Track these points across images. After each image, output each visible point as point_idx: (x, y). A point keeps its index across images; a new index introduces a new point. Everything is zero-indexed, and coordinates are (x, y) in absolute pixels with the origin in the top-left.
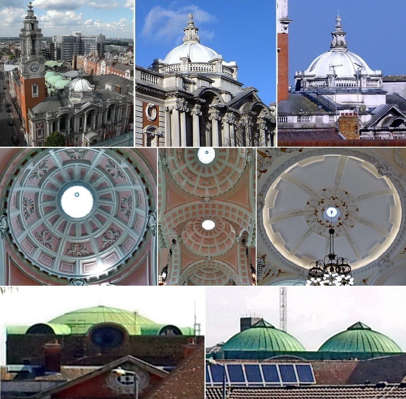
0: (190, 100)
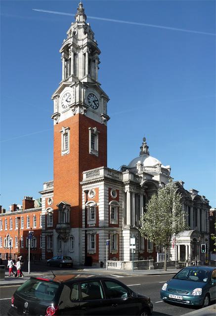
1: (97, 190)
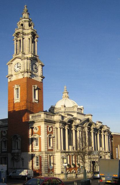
0: (64, 124)
1: (40, 127)
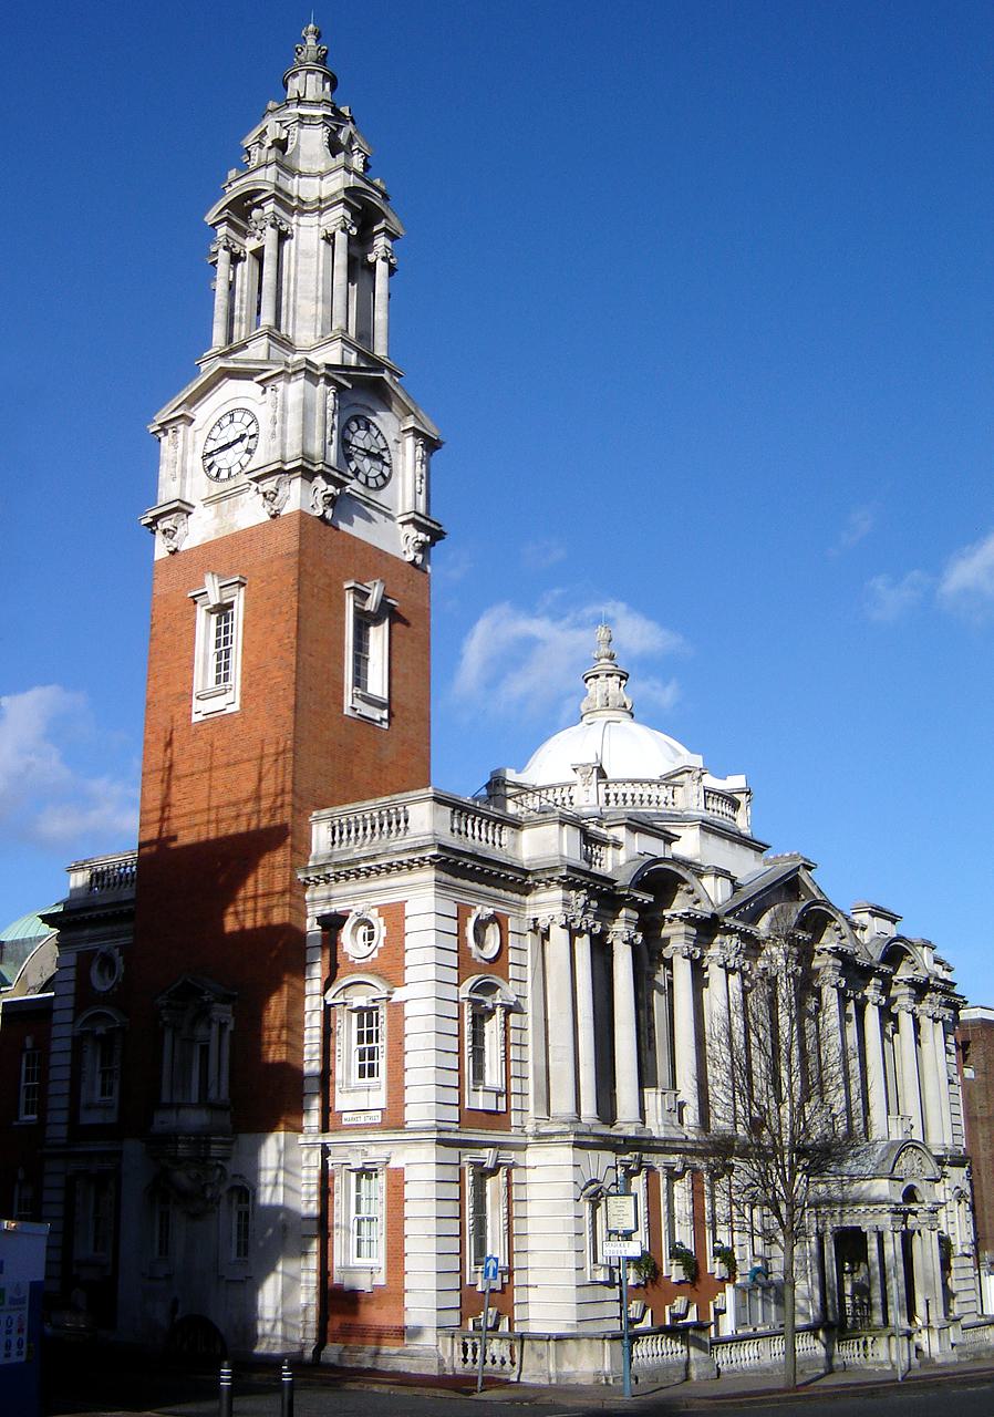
0: (605, 896)
